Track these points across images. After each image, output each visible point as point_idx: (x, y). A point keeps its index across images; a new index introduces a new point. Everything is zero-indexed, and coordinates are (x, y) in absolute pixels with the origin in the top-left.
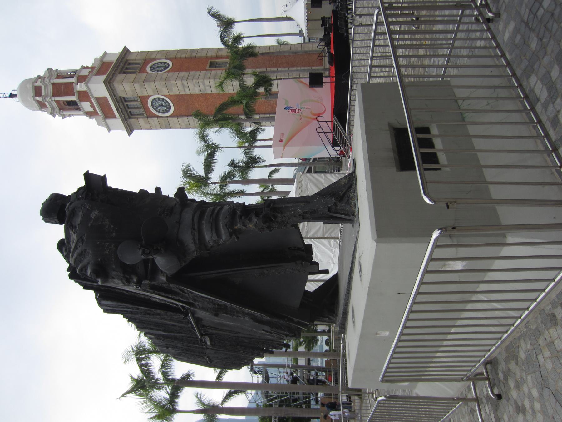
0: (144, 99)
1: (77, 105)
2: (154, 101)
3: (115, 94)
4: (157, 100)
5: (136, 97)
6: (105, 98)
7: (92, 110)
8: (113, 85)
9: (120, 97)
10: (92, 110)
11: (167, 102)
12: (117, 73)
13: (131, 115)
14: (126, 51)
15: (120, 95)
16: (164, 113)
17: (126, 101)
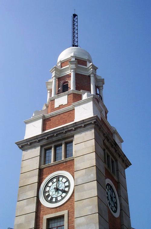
0: (69, 165)
1: (64, 91)
2: (64, 180)
3: (79, 130)
4: (67, 184)
5: (72, 155)
6: (73, 121)
7: (56, 105)
8: (91, 128)
9: (73, 136)
10: (56, 105)
11: (63, 198)
12: (106, 141)
13: (46, 150)
14: (127, 164)
15: (75, 137)
16: (45, 192)
17: (66, 144)
